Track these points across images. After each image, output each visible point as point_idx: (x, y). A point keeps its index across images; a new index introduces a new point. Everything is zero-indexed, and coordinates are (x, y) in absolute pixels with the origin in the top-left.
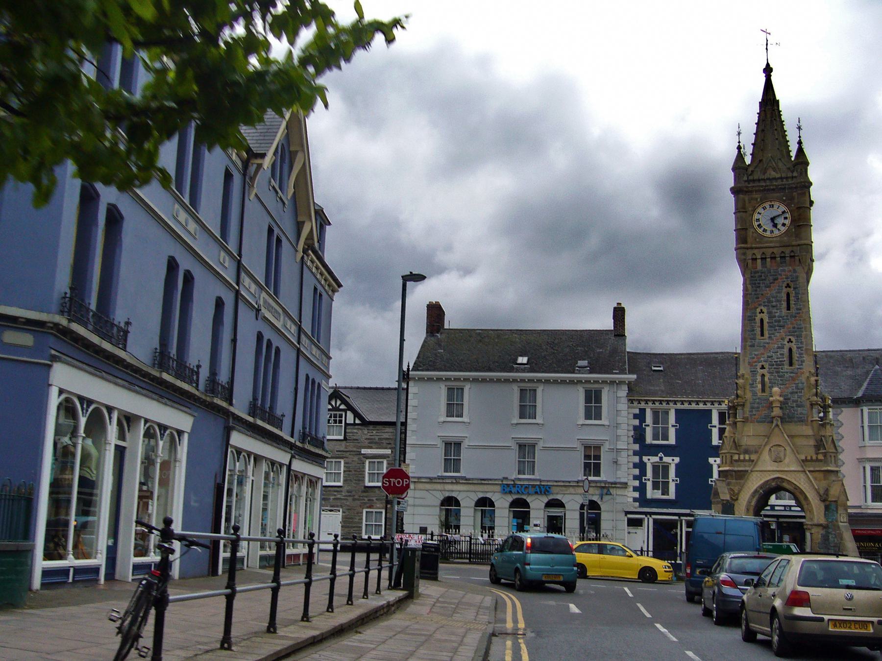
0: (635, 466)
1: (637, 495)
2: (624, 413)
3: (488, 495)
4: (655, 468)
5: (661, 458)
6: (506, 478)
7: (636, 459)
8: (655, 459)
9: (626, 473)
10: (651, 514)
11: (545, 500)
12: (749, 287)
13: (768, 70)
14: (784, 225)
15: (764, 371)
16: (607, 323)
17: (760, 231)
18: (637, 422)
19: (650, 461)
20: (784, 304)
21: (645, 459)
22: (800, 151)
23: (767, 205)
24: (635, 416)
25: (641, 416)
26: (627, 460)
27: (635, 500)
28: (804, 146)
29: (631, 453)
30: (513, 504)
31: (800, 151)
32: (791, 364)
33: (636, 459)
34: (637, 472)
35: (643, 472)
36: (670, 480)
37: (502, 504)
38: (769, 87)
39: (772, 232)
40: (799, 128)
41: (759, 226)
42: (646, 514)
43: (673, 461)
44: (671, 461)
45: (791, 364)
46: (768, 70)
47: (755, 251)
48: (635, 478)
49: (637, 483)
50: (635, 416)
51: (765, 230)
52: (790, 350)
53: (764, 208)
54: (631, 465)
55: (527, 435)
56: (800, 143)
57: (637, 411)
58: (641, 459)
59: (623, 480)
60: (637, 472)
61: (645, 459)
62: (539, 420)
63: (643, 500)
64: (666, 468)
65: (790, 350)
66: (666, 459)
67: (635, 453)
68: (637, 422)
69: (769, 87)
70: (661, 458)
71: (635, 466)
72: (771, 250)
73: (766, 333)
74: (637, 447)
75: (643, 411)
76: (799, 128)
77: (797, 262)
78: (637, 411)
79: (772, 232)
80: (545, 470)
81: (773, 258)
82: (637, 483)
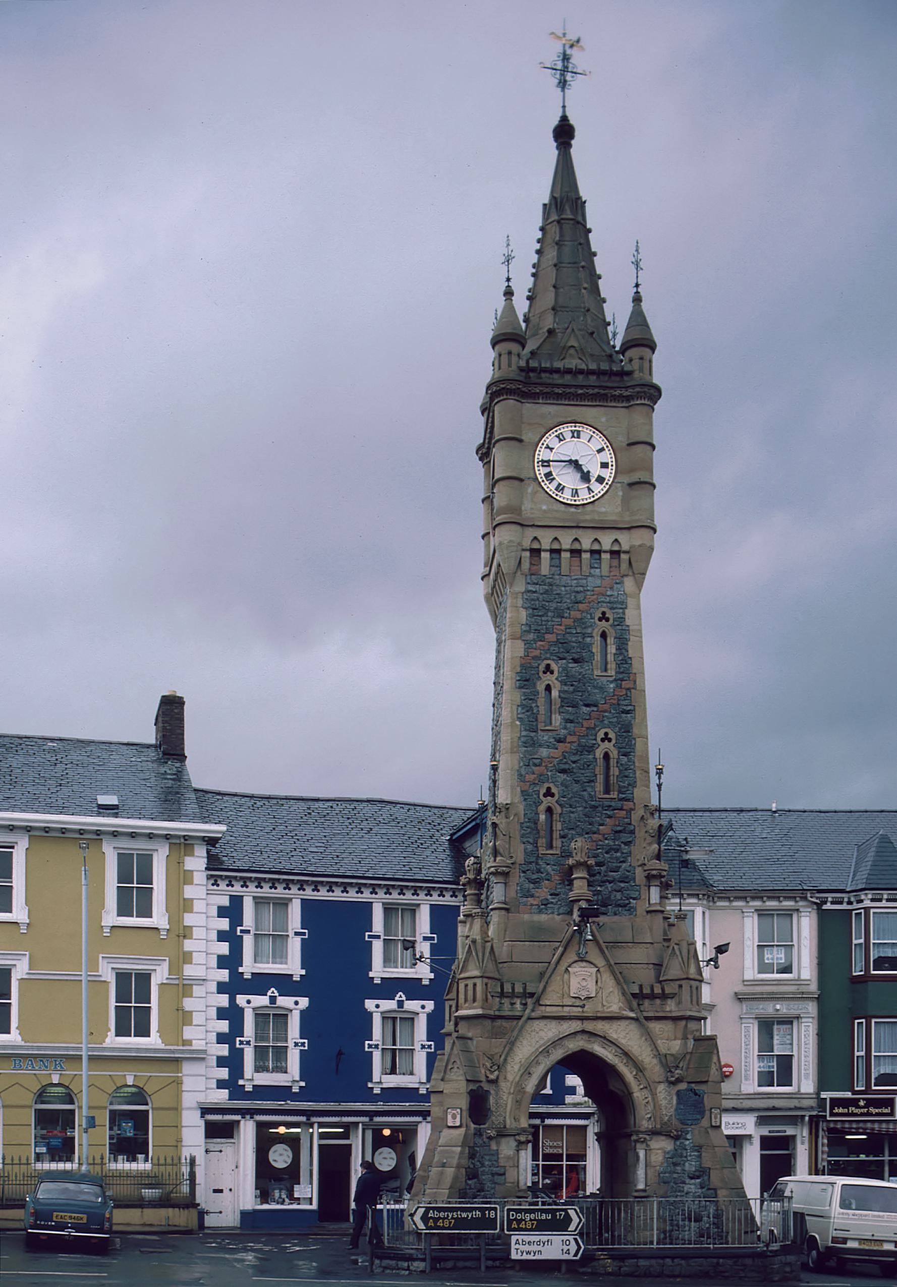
7: (224, 1000)
8: (261, 1001)
13: (564, 133)
14: (600, 480)
17: (551, 488)
19: (251, 1003)
21: (241, 1000)
22: (638, 319)
23: (566, 430)
26: (205, 1003)
28: (644, 305)
31: (638, 319)
33: (224, 1000)
38: (565, 171)
39: (575, 493)
40: (637, 264)
41: (548, 475)
44: (292, 1006)
46: (564, 133)
47: (538, 533)
51: (560, 488)
53: (561, 438)
56: (637, 299)
58: (232, 1000)
61: (241, 1000)
67: (222, 988)
69: (565, 171)
74: (224, 975)
76: (637, 264)
77: (624, 566)
79: (575, 493)
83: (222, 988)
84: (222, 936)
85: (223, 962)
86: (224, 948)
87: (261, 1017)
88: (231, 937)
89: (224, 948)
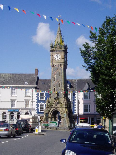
0: (36, 105)
1: (37, 111)
2: (34, 94)
3: (5, 112)
4: (41, 105)
5: (42, 103)
6: (9, 108)
7: (37, 104)
8: (41, 103)
9: (35, 107)
10: (40, 115)
11: (17, 113)
12: (53, 71)
15: (55, 88)
16: (34, 72)
18: (37, 96)
19: (39, 104)
20: (59, 74)
21: (38, 103)
24: (37, 94)
25: (38, 94)
27: (36, 112)
29: (36, 102)
30: (10, 114)
32: (60, 86)
33: (37, 104)
34: (37, 106)
35: (38, 106)
36: (44, 108)
37: (8, 114)
42: (39, 115)
43: (44, 104)
45: (60, 86)
48: (36, 107)
49: (37, 109)
50: (37, 94)
52: (60, 83)
54: (35, 105)
55: (13, 98)
57: (37, 93)
58: (38, 103)
59: (34, 108)
60: (37, 106)
61: (38, 103)
62: (16, 95)
63: (38, 112)
64: (43, 105)
65: (60, 83)
66: (43, 104)
67: (36, 102)
68: (37, 96)
70: (42, 103)
71: (36, 105)
72: (57, 63)
73: (55, 80)
74: (37, 101)
75: (38, 93)
78: (37, 93)
80: (17, 106)
81: (57, 65)
82: (37, 109)
83: (36, 102)
84: (37, 97)
85: (37, 100)
86: (37, 98)
87: (41, 105)
88: (37, 97)
89: (37, 98)
